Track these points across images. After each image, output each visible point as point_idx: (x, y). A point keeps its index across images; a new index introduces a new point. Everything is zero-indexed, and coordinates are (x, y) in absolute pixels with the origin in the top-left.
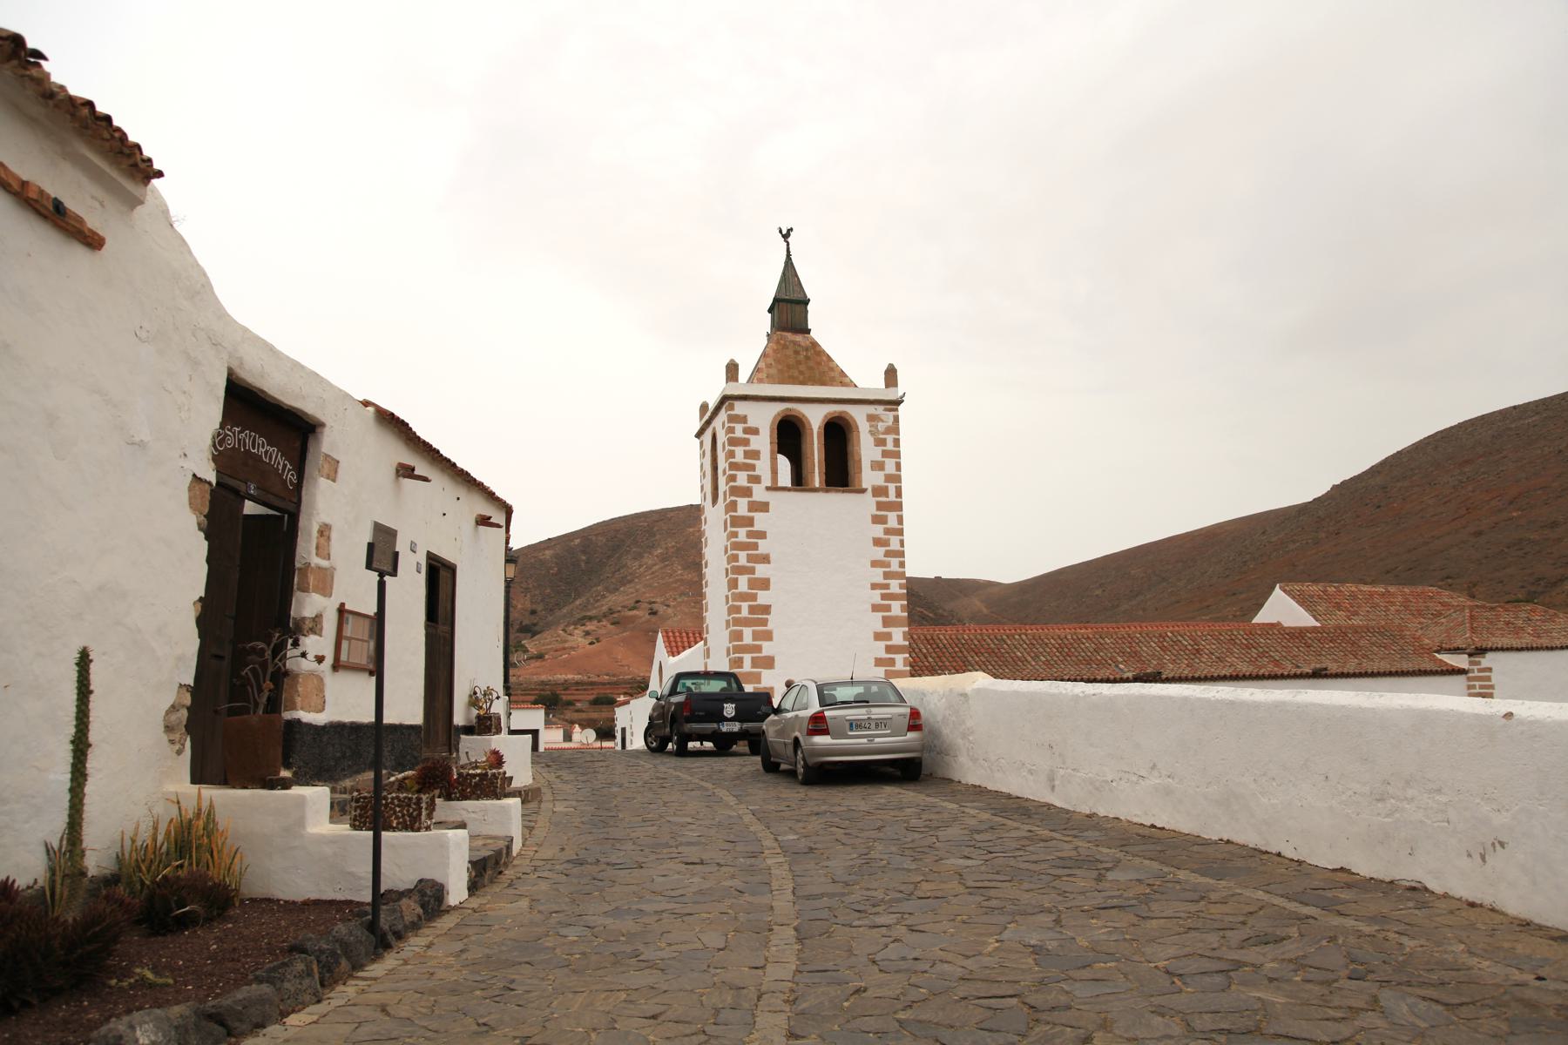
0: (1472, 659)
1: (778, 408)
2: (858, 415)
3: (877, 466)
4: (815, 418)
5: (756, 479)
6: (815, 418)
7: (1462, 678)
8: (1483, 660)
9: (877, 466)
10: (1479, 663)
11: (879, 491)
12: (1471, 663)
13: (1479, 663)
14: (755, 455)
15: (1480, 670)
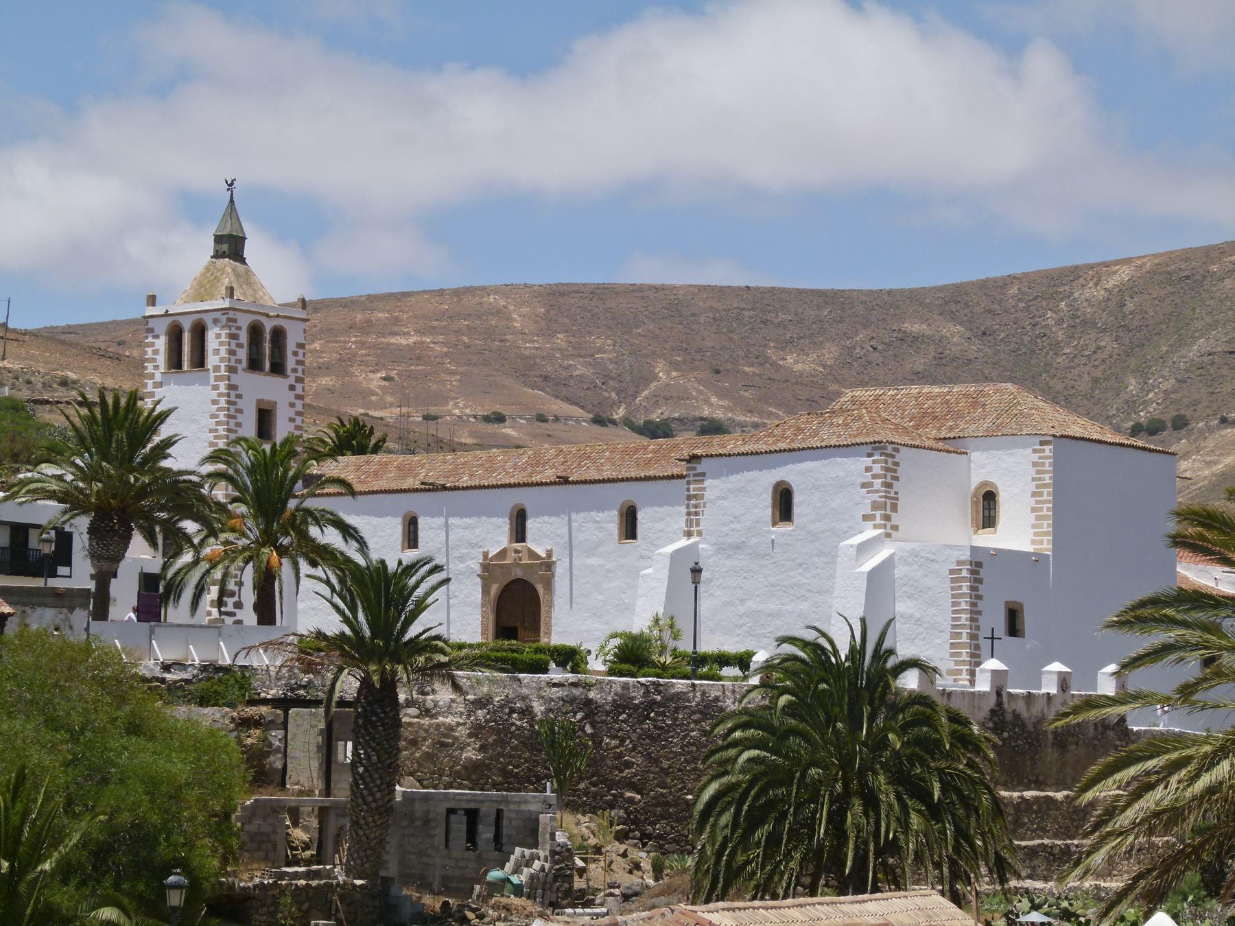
0: (689, 465)
1: (170, 320)
2: (208, 319)
3: (217, 352)
4: (187, 324)
5: (156, 367)
6: (187, 324)
7: (684, 481)
8: (698, 466)
9: (217, 352)
10: (695, 469)
11: (217, 369)
12: (689, 469)
13: (695, 469)
14: (156, 352)
15: (695, 475)
